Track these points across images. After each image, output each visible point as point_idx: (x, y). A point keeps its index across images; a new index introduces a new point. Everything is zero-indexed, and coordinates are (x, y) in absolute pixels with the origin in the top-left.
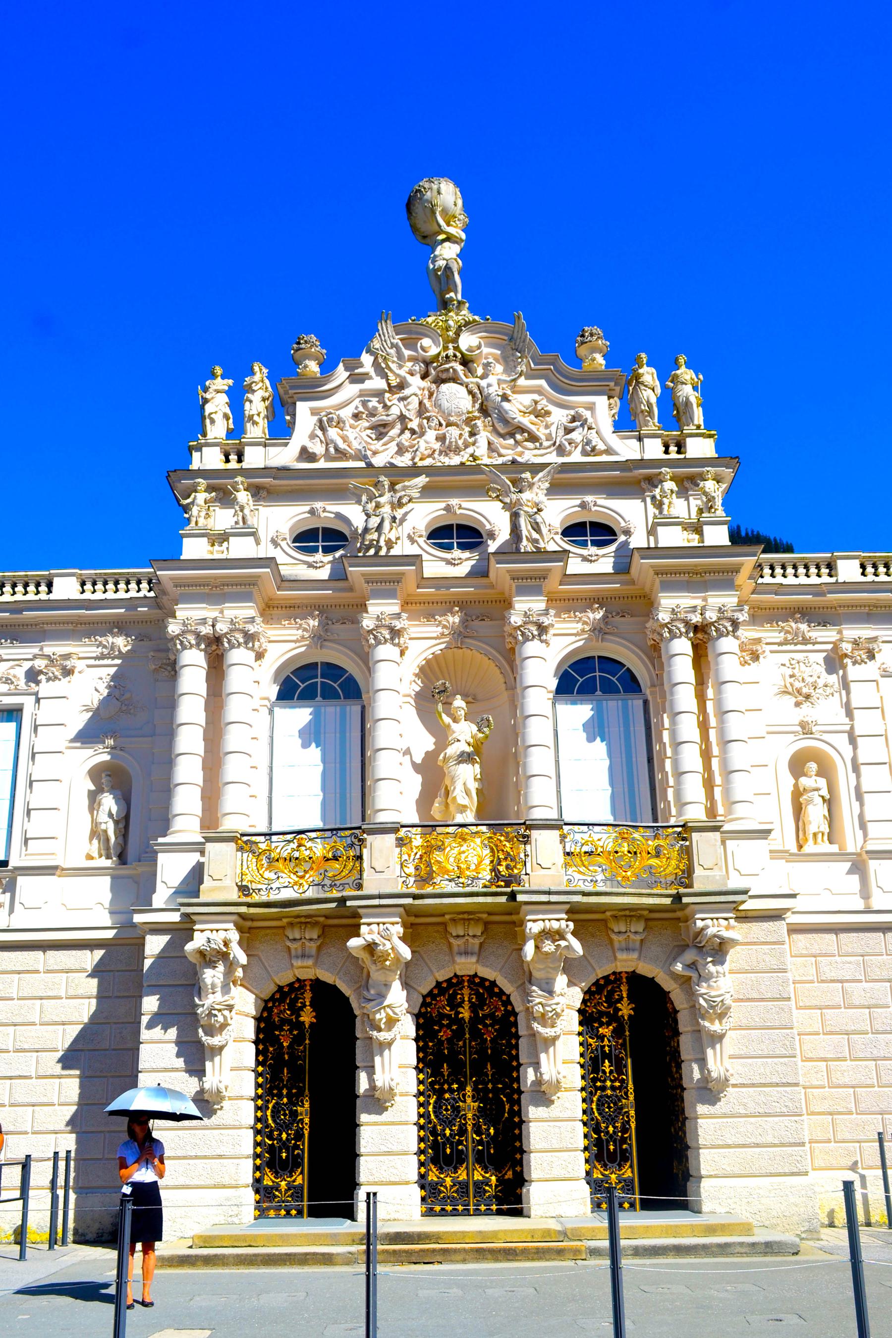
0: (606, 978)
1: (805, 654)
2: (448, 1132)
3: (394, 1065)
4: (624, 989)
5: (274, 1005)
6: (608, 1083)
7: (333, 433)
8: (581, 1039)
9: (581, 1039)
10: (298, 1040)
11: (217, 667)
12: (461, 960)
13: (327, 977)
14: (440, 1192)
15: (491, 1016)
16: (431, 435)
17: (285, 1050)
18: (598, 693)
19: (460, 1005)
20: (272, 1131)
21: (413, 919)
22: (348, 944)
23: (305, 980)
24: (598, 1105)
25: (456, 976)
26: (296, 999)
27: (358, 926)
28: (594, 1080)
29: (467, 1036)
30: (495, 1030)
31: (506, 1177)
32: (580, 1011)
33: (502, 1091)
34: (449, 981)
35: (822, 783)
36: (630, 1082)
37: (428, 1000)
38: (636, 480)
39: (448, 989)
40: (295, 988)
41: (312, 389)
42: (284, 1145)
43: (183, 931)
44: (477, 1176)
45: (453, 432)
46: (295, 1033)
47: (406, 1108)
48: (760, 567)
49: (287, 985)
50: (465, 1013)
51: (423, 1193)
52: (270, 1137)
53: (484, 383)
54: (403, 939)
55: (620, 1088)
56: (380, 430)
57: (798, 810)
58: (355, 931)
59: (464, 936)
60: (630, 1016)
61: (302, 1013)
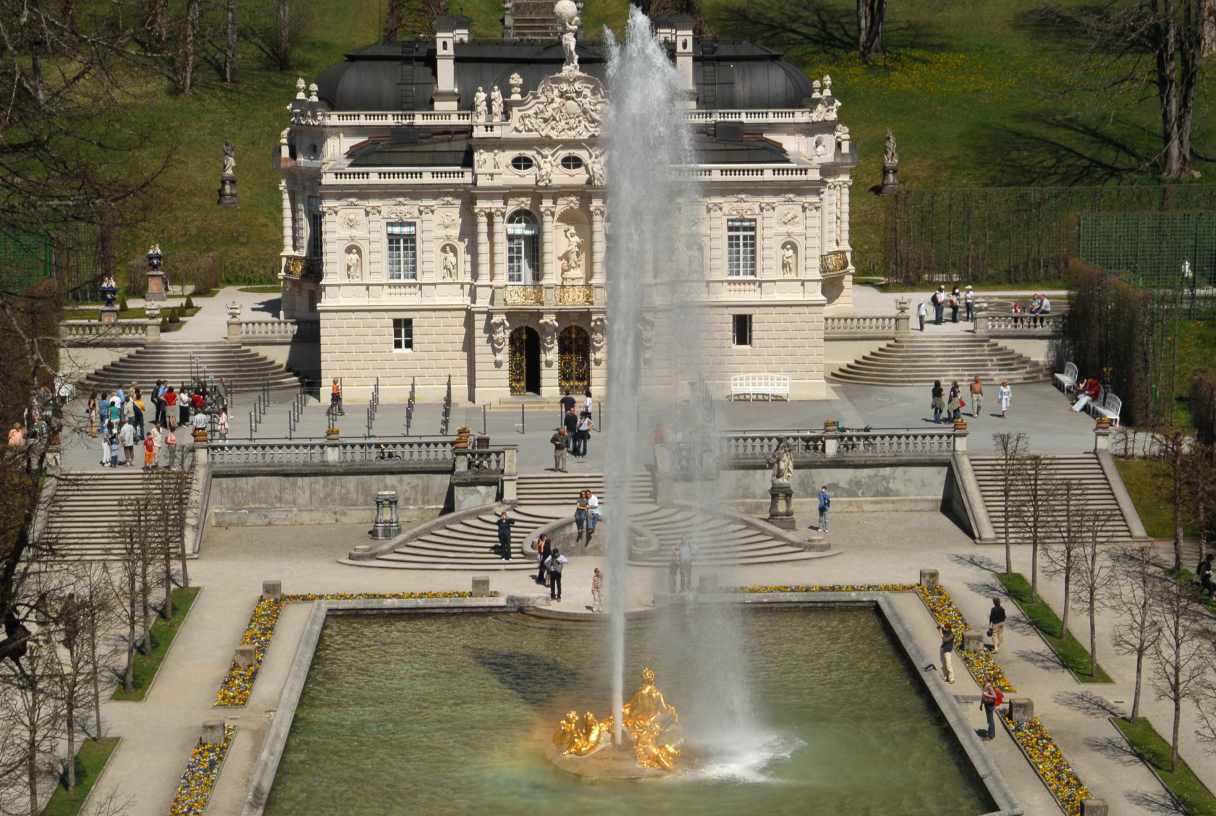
3: (551, 355)
11: (491, 224)
13: (531, 326)
16: (563, 122)
39: (568, 330)
40: (521, 329)
43: (490, 315)
45: (572, 121)
47: (556, 365)
50: (574, 336)
53: (584, 101)
56: (546, 121)
58: (541, 318)
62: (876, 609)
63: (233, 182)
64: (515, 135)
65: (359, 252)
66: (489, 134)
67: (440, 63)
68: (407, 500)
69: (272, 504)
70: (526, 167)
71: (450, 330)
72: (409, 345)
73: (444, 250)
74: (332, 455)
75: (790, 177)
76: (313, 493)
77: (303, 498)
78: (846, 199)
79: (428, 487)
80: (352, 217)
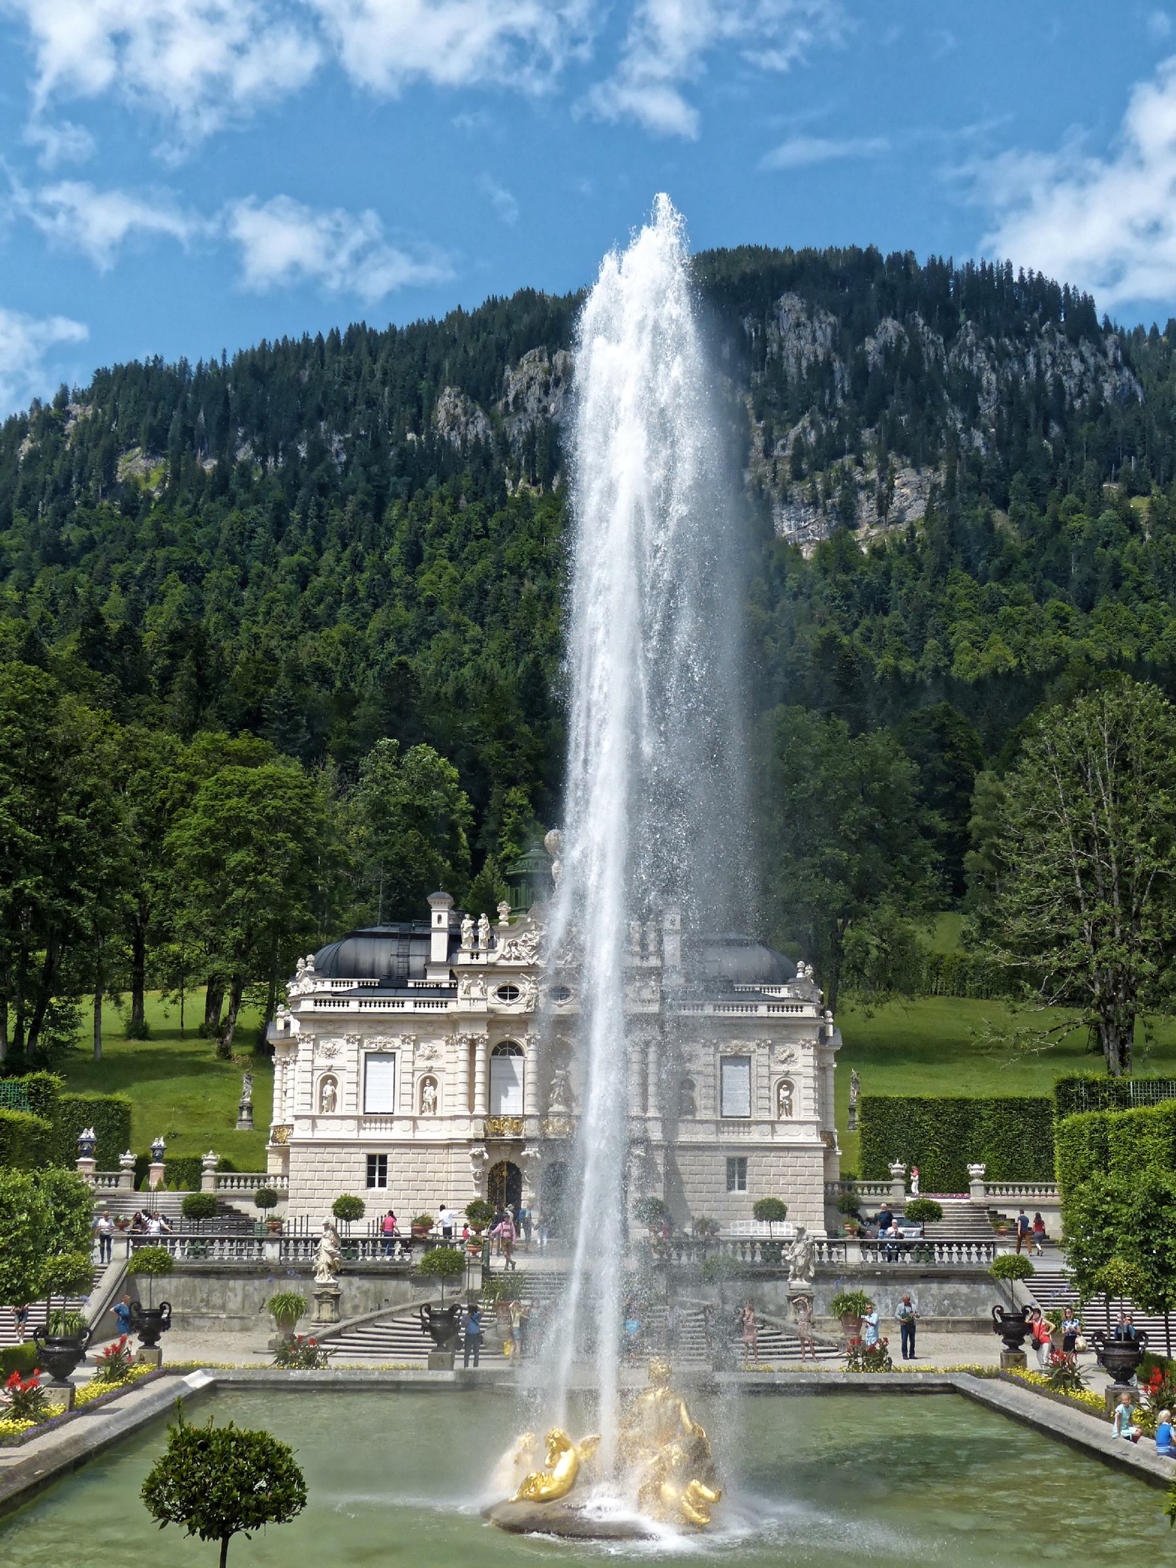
62: (951, 1389)
63: (250, 1109)
64: (503, 963)
65: (335, 1083)
66: (475, 961)
67: (434, 935)
68: (355, 1308)
69: (198, 1308)
70: (512, 997)
71: (429, 1167)
72: (383, 1183)
73: (423, 1084)
74: (272, 1252)
75: (785, 1014)
76: (246, 1296)
77: (234, 1303)
78: (831, 1082)
79: (381, 1293)
80: (329, 1046)
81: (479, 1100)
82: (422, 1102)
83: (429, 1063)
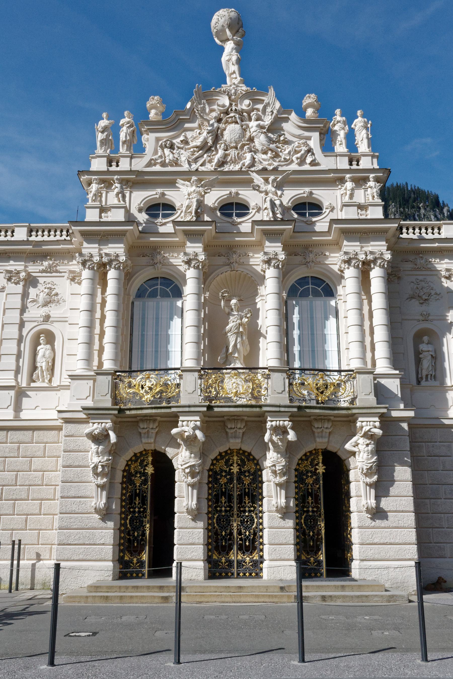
0: (311, 452)
1: (425, 277)
2: (224, 533)
4: (321, 458)
5: (132, 463)
6: (310, 509)
7: (167, 151)
8: (297, 485)
9: (297, 485)
10: (145, 482)
12: (232, 441)
14: (219, 565)
15: (249, 471)
16: (221, 152)
17: (138, 487)
18: (311, 296)
19: (231, 465)
20: (129, 531)
21: (207, 419)
22: (172, 432)
23: (148, 450)
24: (304, 520)
25: (230, 449)
26: (144, 460)
27: (178, 422)
28: (303, 507)
29: (235, 482)
30: (251, 479)
31: (255, 558)
32: (296, 470)
33: (253, 511)
34: (226, 452)
35: (430, 348)
36: (322, 509)
37: (215, 462)
38: (335, 179)
39: (225, 456)
40: (144, 454)
41: (155, 127)
42: (136, 538)
44: (239, 558)
45: (233, 153)
46: (143, 478)
48: (401, 229)
49: (139, 453)
50: (235, 469)
51: (210, 566)
52: (129, 534)
54: (201, 429)
55: (317, 512)
57: (418, 361)
59: (234, 428)
60: (323, 473)
61: (147, 468)
73: (36, 343)
81: (108, 352)
82: (34, 367)
83: (43, 311)
